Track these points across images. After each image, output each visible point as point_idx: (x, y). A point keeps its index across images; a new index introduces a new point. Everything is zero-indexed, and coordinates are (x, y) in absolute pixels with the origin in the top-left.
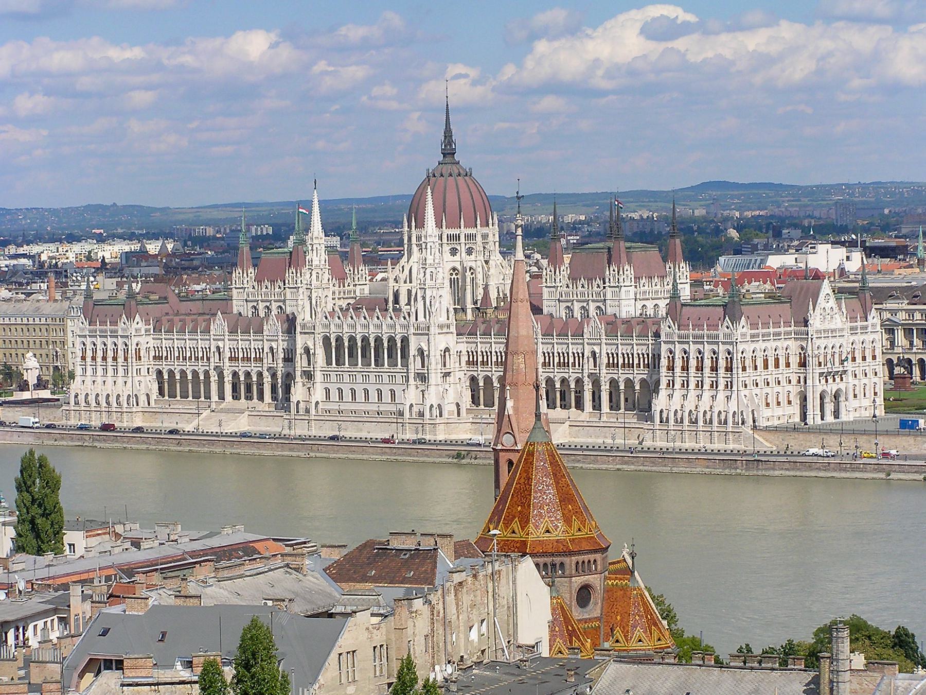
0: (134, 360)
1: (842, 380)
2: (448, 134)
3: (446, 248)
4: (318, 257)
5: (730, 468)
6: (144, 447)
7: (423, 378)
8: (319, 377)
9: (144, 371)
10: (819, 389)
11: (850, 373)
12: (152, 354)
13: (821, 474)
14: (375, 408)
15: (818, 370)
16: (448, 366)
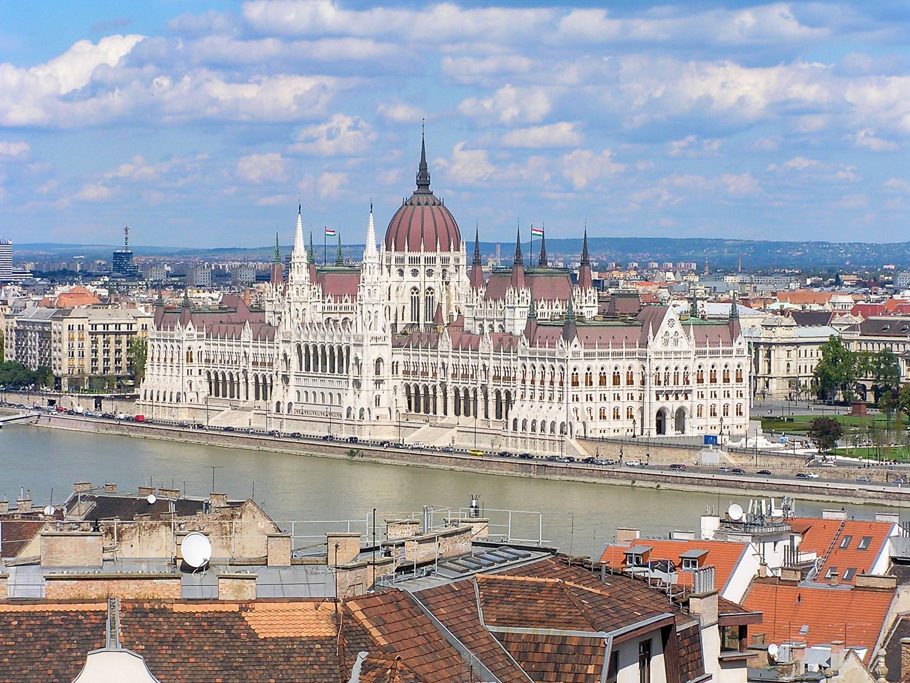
0: (185, 361)
1: (686, 398)
2: (423, 166)
3: (407, 270)
4: (300, 275)
5: (526, 471)
6: (158, 437)
7: (357, 384)
8: (292, 379)
9: (195, 372)
10: (657, 406)
11: (695, 393)
12: (204, 357)
13: (588, 479)
14: (323, 409)
15: (655, 388)
16: (381, 374)
